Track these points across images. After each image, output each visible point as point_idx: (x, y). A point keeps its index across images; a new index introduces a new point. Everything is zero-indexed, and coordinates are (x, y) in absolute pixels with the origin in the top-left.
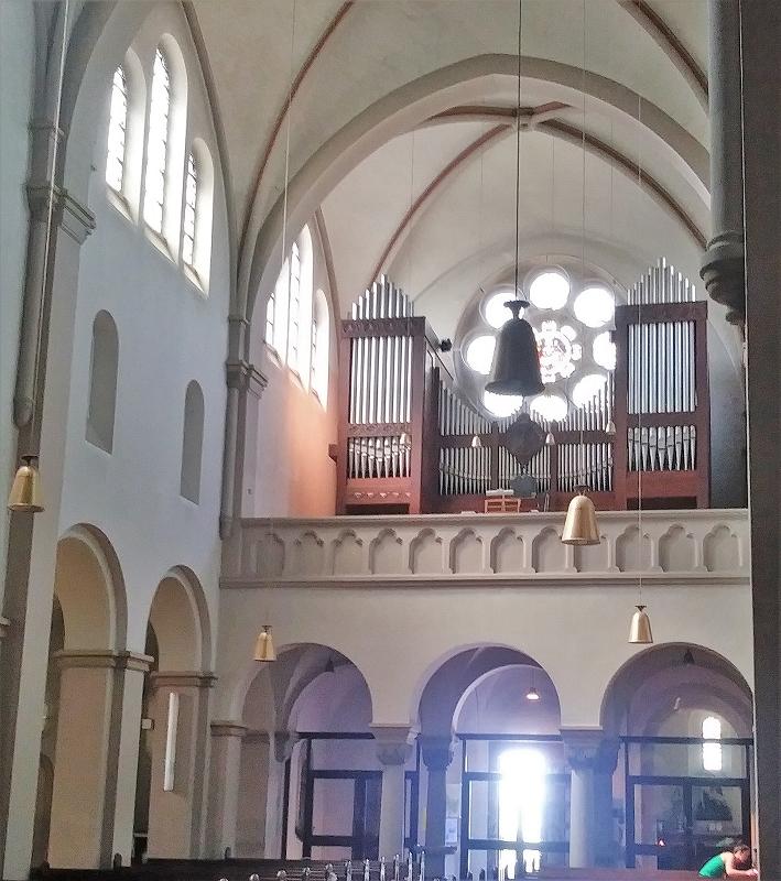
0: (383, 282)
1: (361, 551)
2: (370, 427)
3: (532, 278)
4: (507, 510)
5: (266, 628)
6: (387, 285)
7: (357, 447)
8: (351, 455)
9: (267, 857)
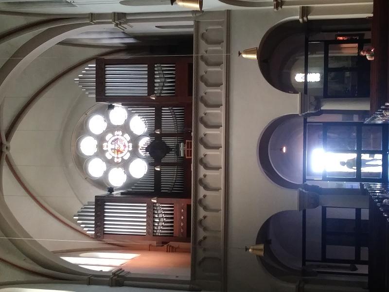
0: (77, 218)
1: (212, 219)
2: (148, 225)
3: (82, 154)
4: (191, 147)
5: (247, 249)
6: (79, 216)
7: (158, 231)
8: (161, 235)
9: (367, 281)
